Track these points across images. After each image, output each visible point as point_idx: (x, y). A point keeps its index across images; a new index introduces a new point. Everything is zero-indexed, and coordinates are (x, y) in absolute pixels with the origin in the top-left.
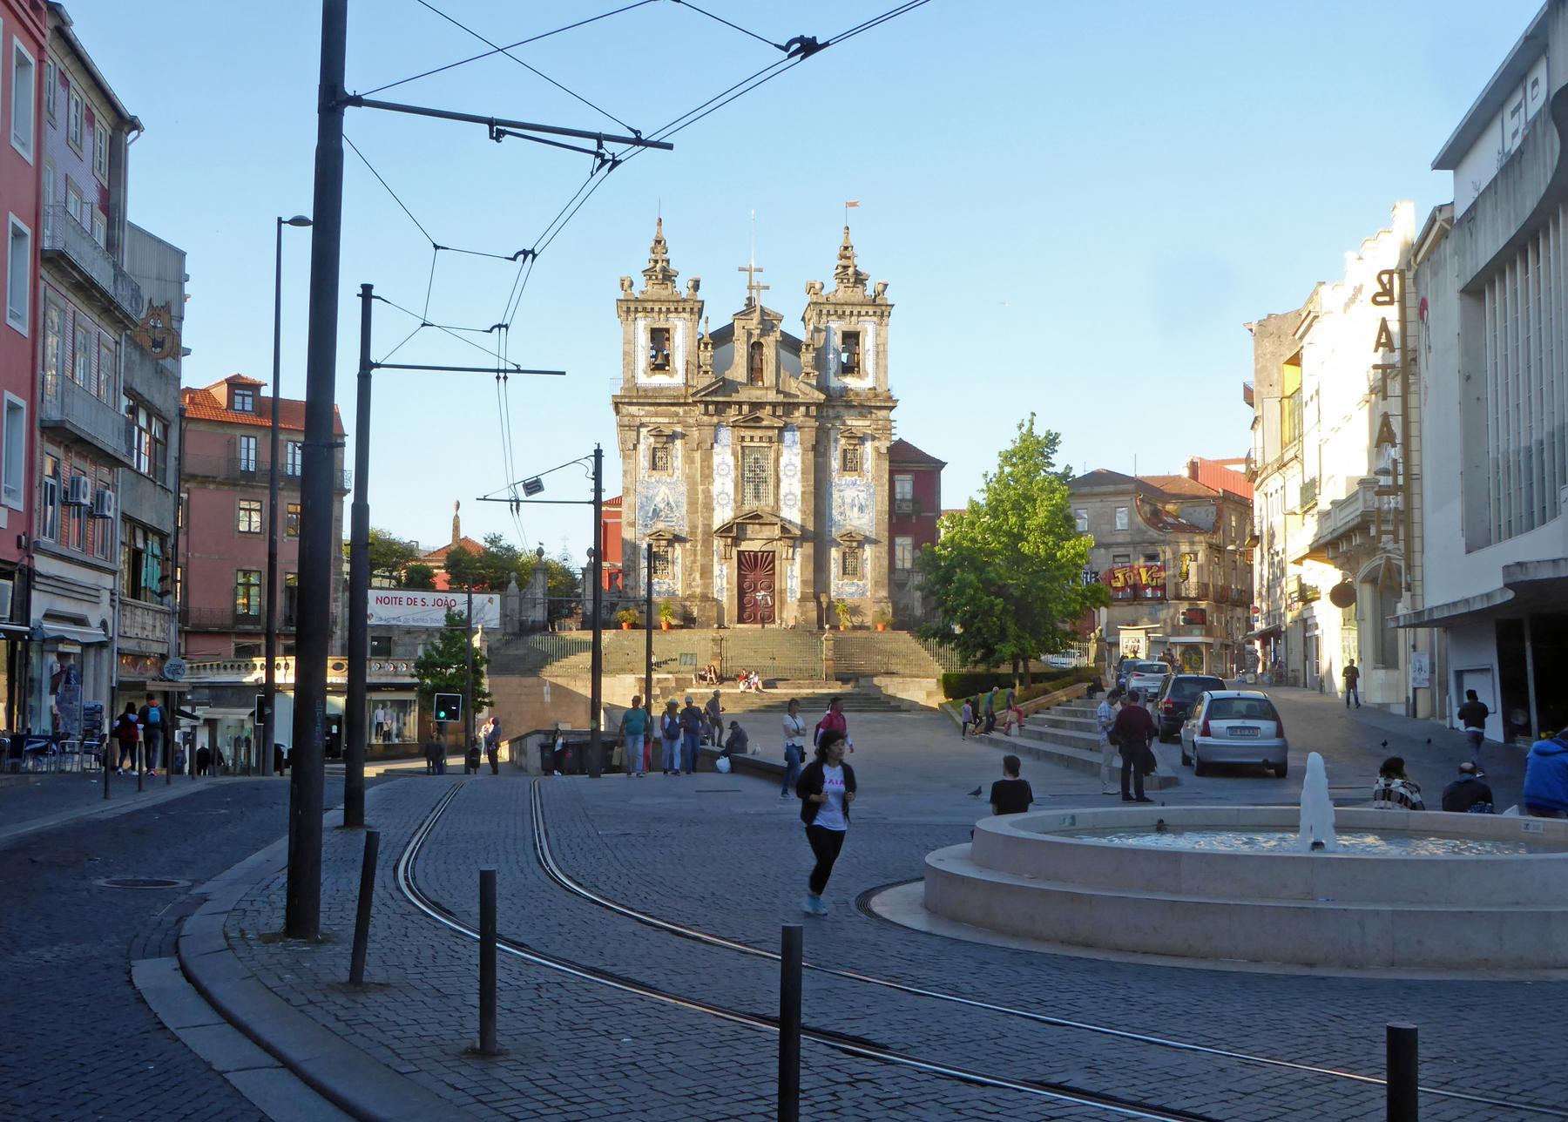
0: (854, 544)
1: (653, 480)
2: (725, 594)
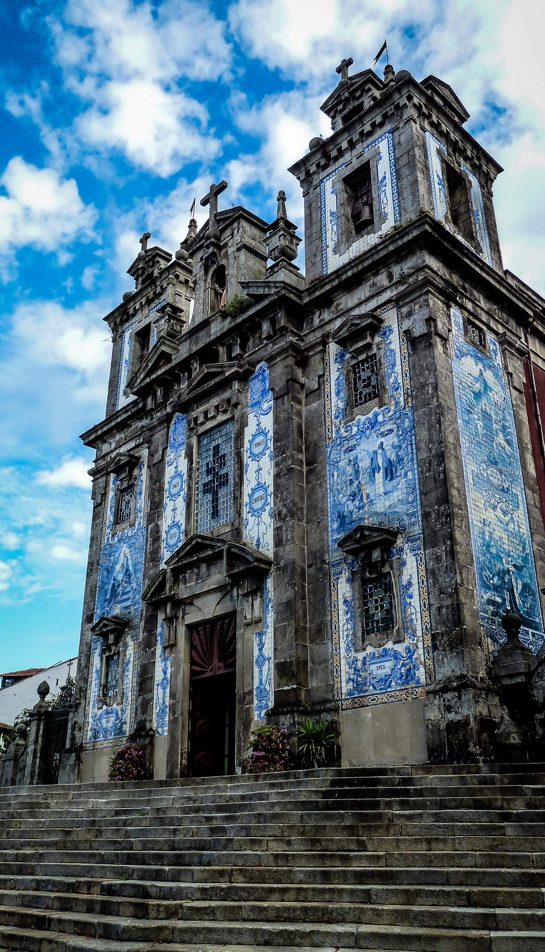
0: (376, 555)
1: (116, 539)
2: (167, 719)
